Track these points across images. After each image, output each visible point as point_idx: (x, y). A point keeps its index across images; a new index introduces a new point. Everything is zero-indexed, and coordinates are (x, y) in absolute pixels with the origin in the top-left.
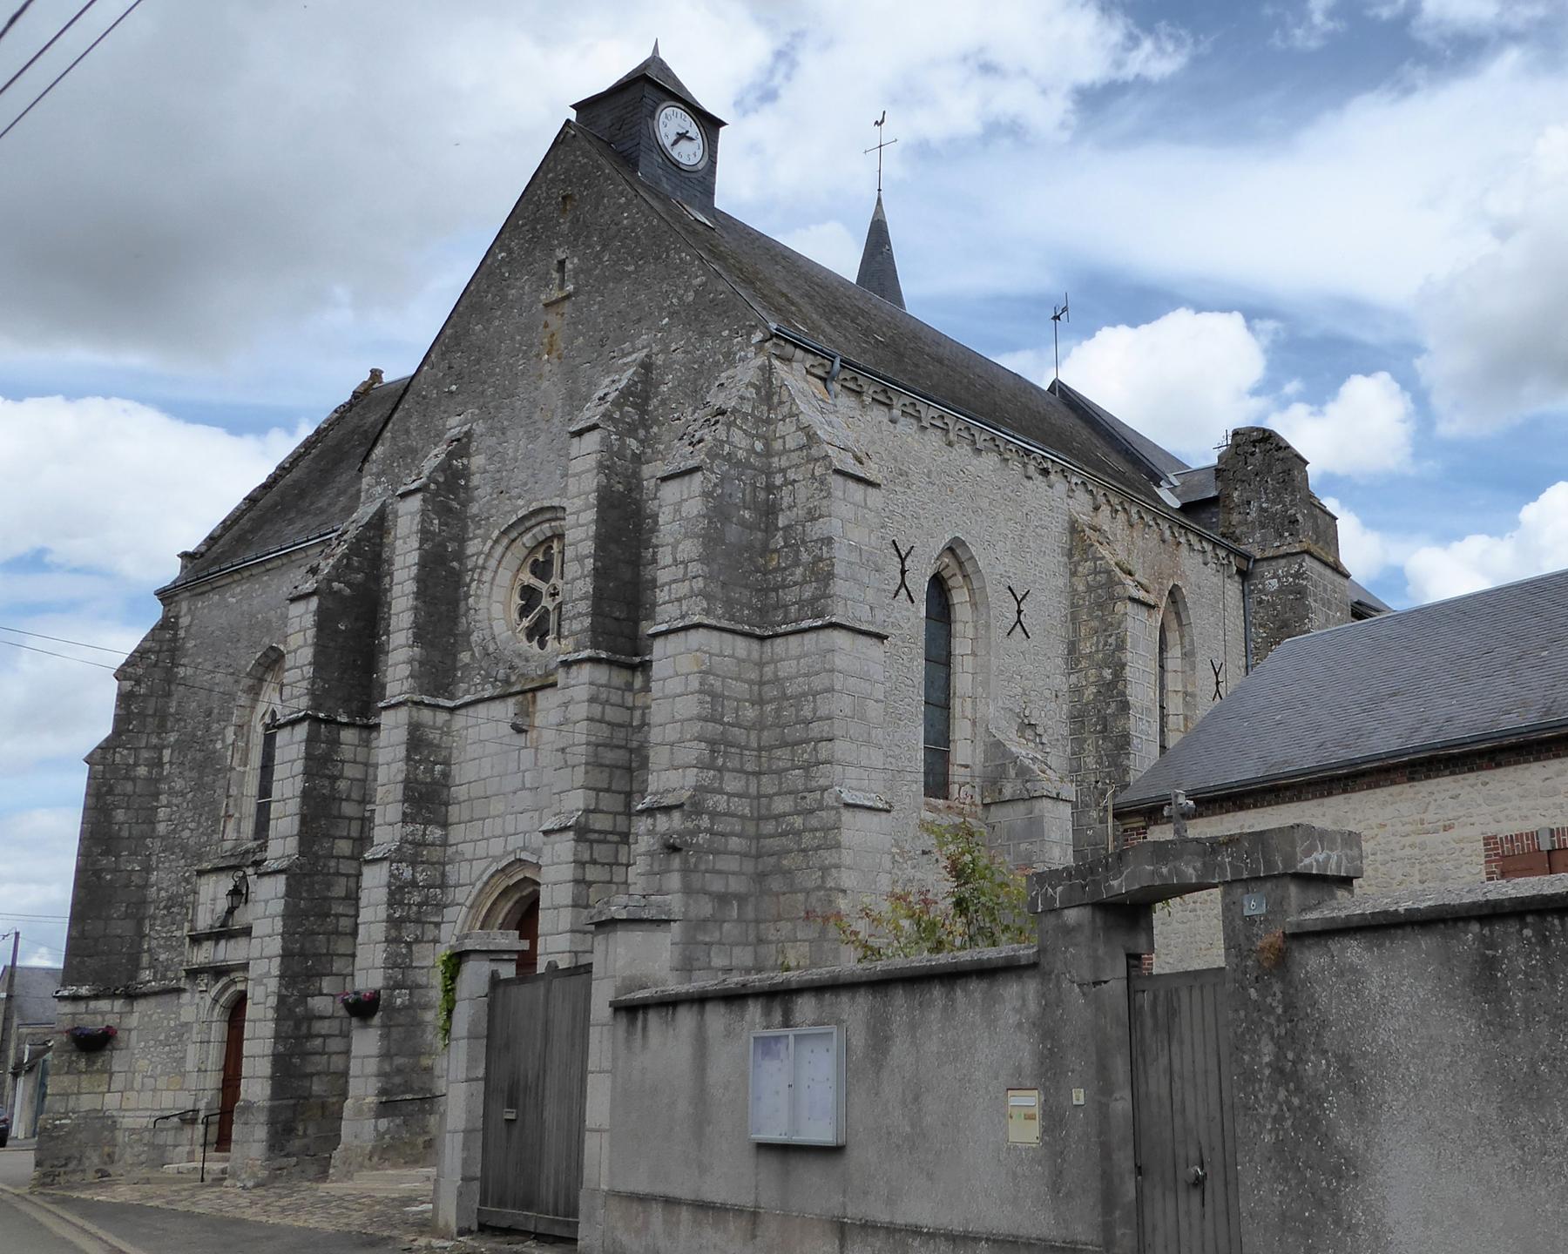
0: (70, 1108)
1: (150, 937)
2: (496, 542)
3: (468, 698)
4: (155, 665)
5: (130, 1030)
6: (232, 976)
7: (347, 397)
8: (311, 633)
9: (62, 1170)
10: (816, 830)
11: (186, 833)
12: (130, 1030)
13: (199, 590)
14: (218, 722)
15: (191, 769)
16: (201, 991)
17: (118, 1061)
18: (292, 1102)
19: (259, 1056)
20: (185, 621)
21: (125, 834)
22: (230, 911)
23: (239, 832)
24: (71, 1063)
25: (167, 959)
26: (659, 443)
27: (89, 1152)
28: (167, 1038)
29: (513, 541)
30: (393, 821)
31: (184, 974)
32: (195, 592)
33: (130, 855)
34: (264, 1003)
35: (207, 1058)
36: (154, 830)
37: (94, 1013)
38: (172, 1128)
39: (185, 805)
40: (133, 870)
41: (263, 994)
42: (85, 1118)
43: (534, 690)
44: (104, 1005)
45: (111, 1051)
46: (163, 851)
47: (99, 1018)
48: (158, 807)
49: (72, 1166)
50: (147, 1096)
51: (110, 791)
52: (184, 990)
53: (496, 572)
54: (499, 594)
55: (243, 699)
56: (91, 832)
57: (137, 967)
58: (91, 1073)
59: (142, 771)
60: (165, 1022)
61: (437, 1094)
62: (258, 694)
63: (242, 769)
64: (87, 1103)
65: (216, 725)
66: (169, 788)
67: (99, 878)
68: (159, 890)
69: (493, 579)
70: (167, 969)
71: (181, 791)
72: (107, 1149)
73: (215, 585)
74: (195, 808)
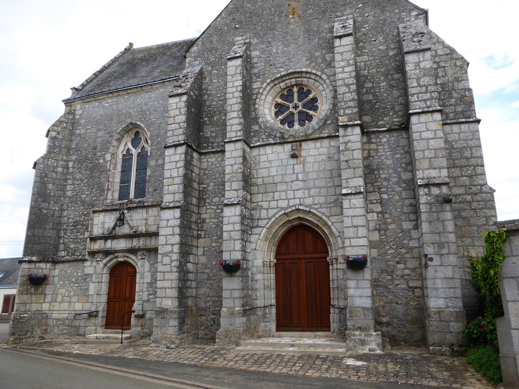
0: (27, 309)
1: (64, 238)
2: (268, 84)
3: (258, 144)
4: (66, 128)
5: (54, 277)
6: (116, 255)
7: (123, 50)
8: (183, 111)
9: (24, 336)
10: (480, 201)
11: (84, 196)
12: (54, 277)
13: (87, 100)
14: (101, 152)
15: (85, 170)
16: (97, 261)
17: (49, 290)
18: (184, 309)
19: (169, 288)
20: (79, 112)
21: (52, 194)
22: (114, 228)
23: (113, 196)
24: (27, 290)
25: (75, 247)
26: (365, 49)
27: (36, 328)
28: (76, 280)
29: (275, 85)
30: (237, 188)
31: (87, 253)
32: (85, 101)
33: (54, 203)
34: (170, 265)
35: (101, 289)
36: (64, 194)
37: (38, 269)
38: (83, 319)
39: (83, 184)
40: (55, 210)
41: (169, 261)
42: (34, 314)
43: (301, 141)
44: (42, 265)
45: (45, 285)
46: (70, 203)
47: (40, 271)
48: (66, 185)
49: (29, 334)
50: (65, 306)
51: (46, 176)
52: (86, 260)
53: (266, 97)
54: (267, 106)
55: (115, 143)
56: (38, 192)
57: (57, 250)
58: (37, 294)
59: (60, 169)
60: (75, 274)
61: (255, 306)
62: (120, 142)
63: (114, 171)
64: (34, 307)
65: (99, 153)
66: (73, 178)
67: (41, 212)
68: (69, 219)
69: (265, 99)
70: (75, 251)
71: (80, 179)
72: (44, 328)
73: (96, 99)
74: (89, 186)
